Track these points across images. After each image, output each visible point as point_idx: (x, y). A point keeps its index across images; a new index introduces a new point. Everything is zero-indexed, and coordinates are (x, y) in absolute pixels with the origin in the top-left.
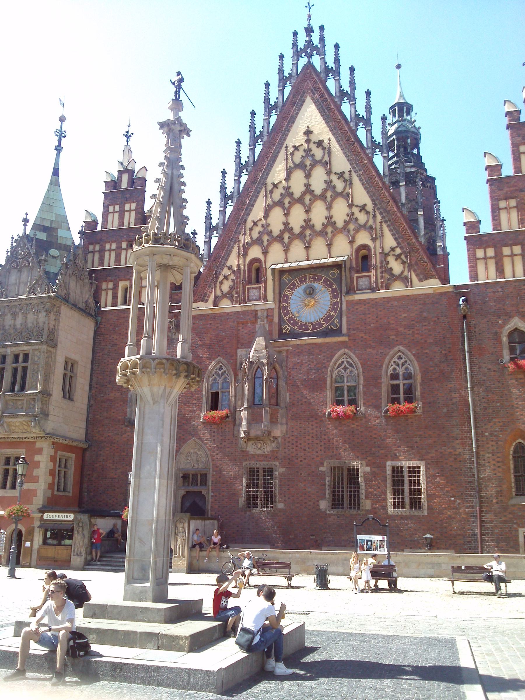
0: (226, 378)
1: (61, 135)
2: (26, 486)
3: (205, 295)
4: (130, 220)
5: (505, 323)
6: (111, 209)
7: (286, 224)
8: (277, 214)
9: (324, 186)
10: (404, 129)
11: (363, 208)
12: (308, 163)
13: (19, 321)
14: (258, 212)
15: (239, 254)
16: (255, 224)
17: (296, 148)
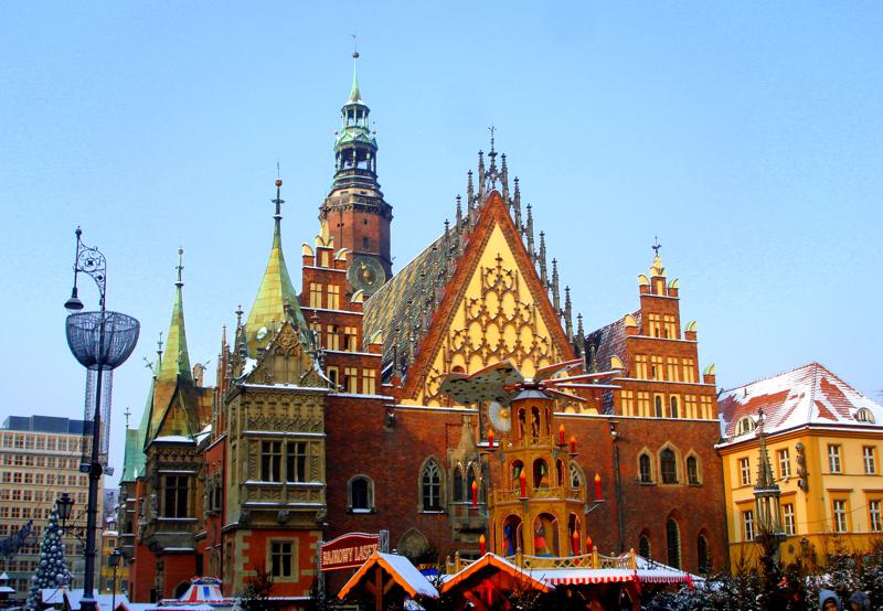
0: (436, 474)
1: (278, 202)
2: (304, 572)
3: (414, 393)
4: (334, 305)
5: (640, 449)
6: (313, 286)
7: (484, 340)
8: (475, 329)
9: (514, 313)
10: (364, 140)
11: (544, 341)
12: (500, 287)
13: (292, 411)
14: (458, 323)
15: (445, 361)
16: (458, 333)
17: (490, 271)
